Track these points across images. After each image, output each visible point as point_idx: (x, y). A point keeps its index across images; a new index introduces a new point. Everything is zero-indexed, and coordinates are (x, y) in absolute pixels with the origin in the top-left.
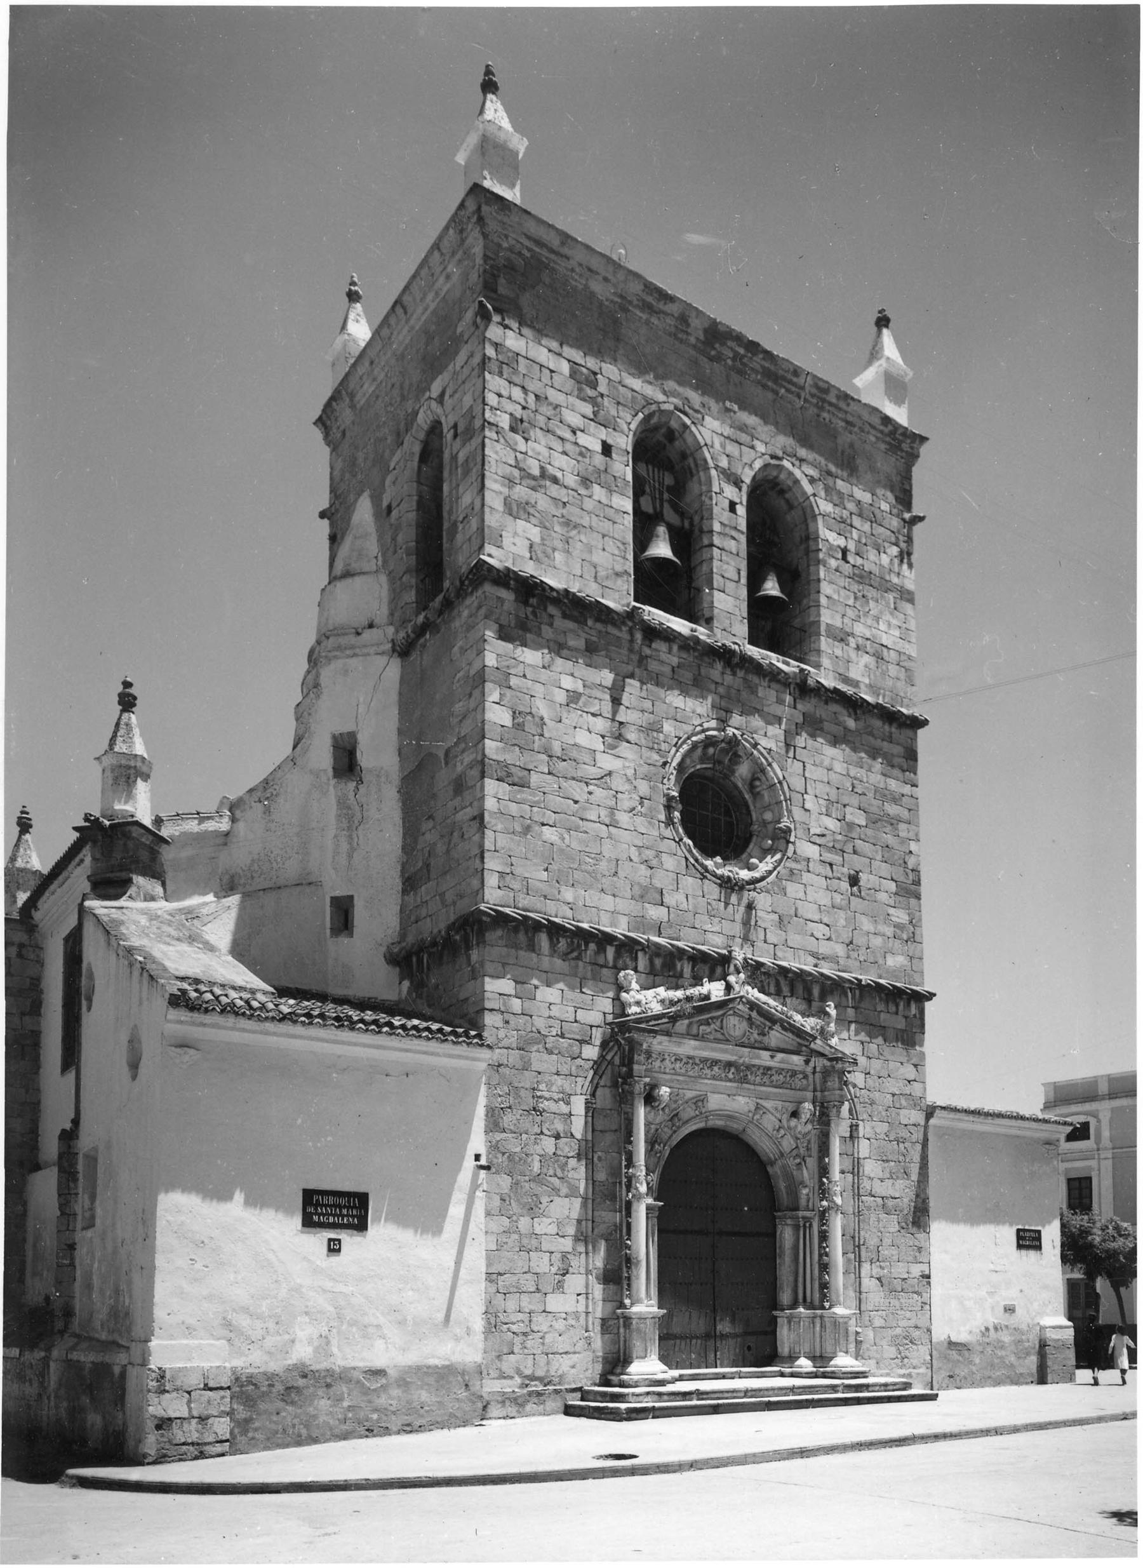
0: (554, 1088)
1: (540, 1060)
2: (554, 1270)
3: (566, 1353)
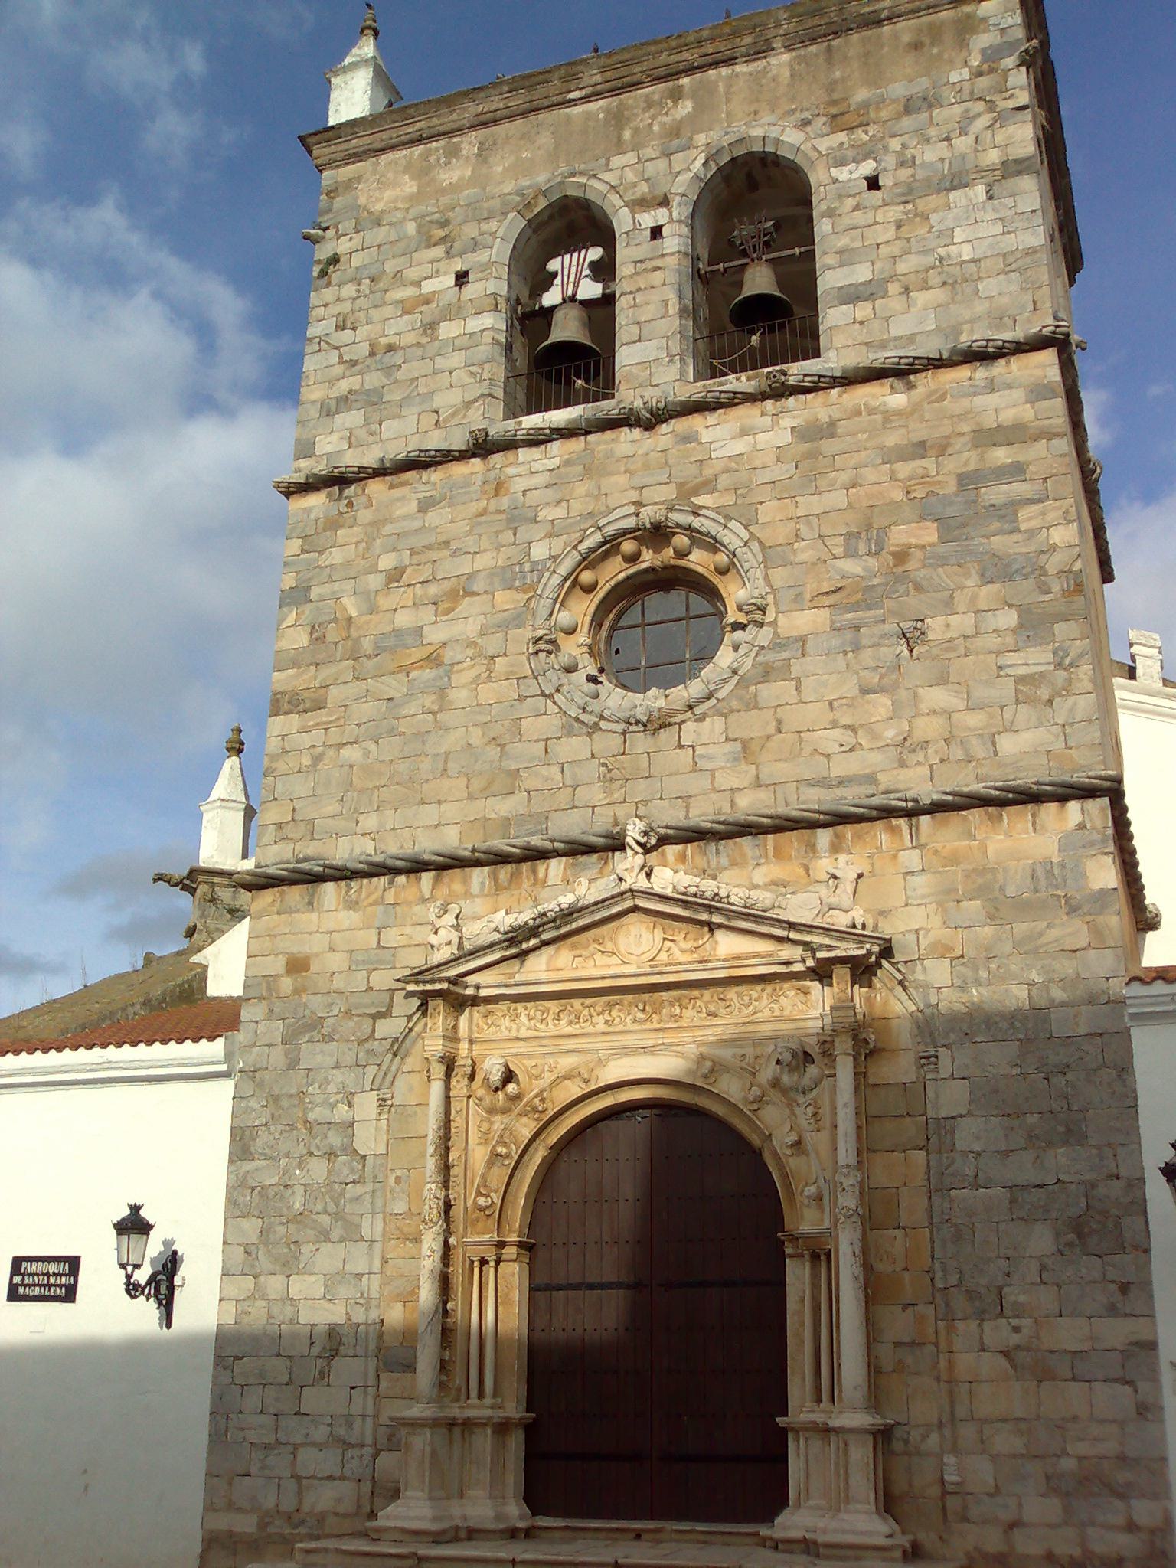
0: (332, 1088)
2: (315, 1350)
3: (330, 1478)
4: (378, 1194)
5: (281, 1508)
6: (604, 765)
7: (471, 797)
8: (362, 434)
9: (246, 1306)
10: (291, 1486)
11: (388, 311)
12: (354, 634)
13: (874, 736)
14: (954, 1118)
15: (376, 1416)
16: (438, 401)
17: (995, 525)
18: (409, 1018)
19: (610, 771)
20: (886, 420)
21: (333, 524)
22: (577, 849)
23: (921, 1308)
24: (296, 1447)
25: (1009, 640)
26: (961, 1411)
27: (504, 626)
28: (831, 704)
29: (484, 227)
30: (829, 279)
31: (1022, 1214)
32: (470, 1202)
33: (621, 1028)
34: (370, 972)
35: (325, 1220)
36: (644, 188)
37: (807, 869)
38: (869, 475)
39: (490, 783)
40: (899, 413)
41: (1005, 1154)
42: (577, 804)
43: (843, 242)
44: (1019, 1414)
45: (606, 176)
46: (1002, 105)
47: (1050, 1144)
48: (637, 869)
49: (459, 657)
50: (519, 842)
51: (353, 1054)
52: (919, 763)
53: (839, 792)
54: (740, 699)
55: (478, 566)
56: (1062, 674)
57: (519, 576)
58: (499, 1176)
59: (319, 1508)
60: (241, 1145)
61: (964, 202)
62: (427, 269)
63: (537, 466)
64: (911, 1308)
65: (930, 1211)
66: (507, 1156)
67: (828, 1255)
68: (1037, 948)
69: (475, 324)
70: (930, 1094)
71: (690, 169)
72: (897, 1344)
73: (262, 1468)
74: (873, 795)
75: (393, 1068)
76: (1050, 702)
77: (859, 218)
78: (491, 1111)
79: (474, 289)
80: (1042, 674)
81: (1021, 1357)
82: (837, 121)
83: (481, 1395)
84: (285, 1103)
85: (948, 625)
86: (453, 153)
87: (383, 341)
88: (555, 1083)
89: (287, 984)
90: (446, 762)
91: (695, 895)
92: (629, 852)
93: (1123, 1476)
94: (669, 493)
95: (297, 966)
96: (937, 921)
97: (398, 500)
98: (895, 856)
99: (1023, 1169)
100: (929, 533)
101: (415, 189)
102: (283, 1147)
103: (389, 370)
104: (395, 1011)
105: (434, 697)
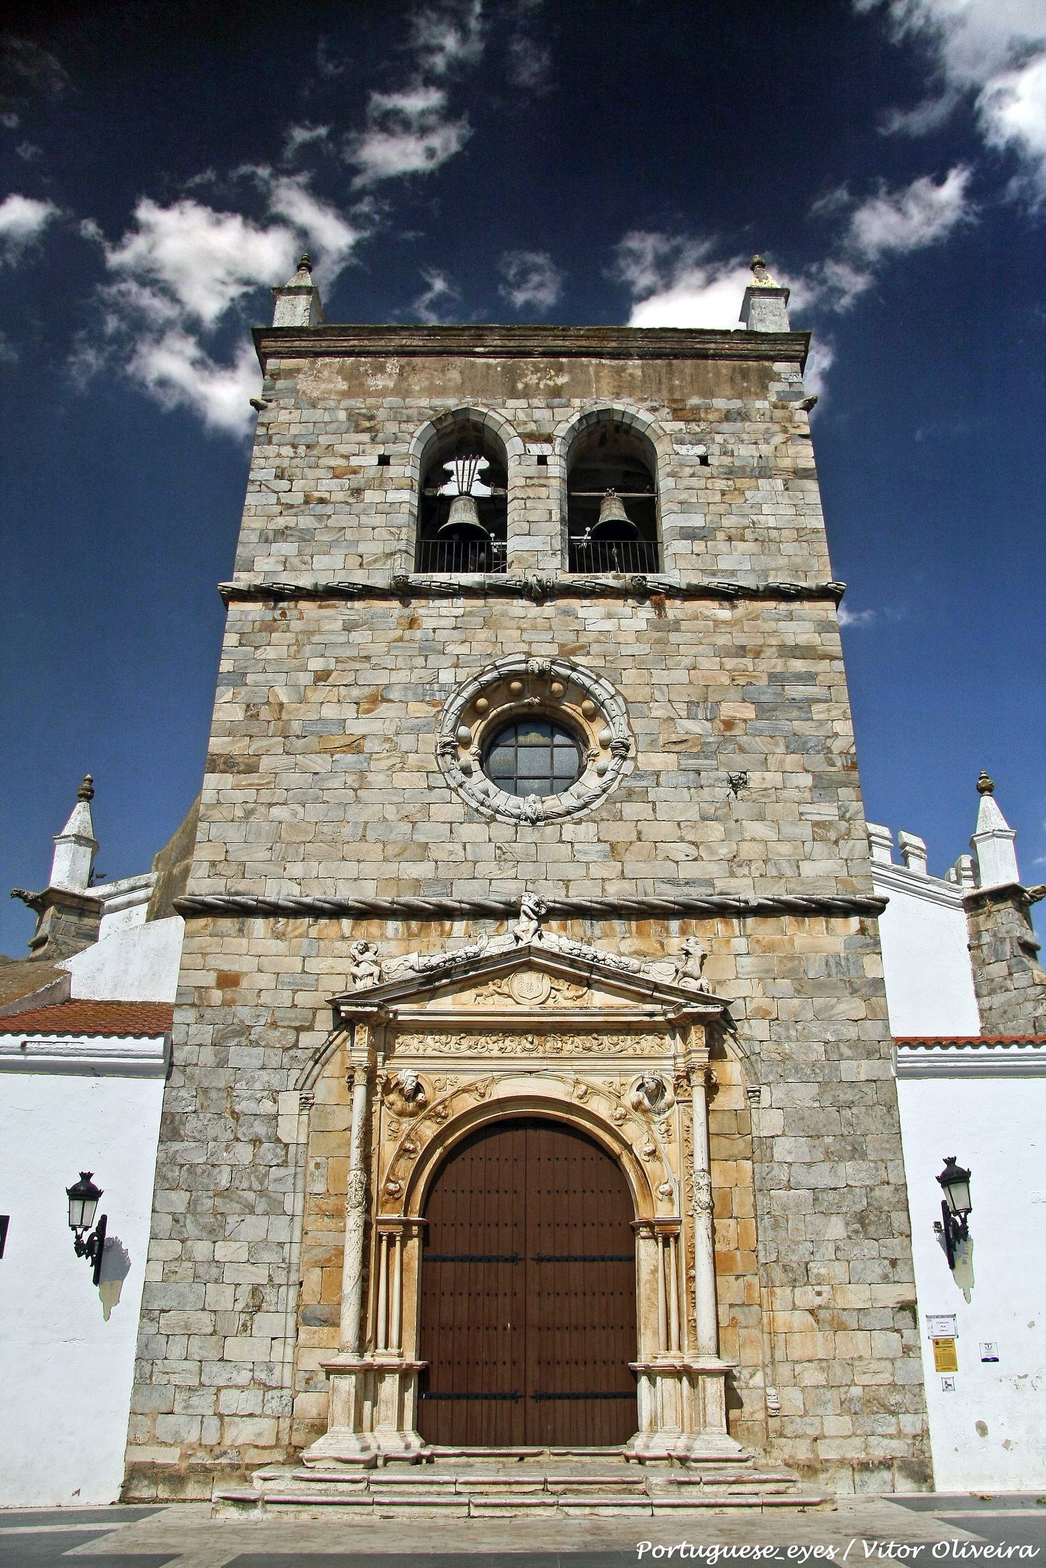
0: (258, 1085)
1: (239, 1055)
2: (239, 1306)
3: (251, 1415)
4: (300, 1176)
5: (204, 1442)
6: (499, 848)
7: (385, 860)
8: (296, 561)
9: (173, 1266)
10: (215, 1422)
11: (320, 473)
12: (285, 716)
13: (712, 852)
14: (773, 1137)
15: (294, 1363)
16: (362, 548)
17: (795, 713)
18: (330, 1033)
19: (504, 853)
20: (715, 626)
21: (269, 627)
22: (479, 912)
23: (749, 1278)
24: (219, 1389)
25: (807, 795)
26: (779, 1355)
27: (415, 730)
28: (679, 825)
29: (404, 426)
30: (668, 521)
31: (822, 1209)
32: (382, 1186)
33: (512, 1055)
34: (295, 992)
35: (250, 1196)
36: (532, 427)
37: (662, 945)
38: (705, 663)
39: (404, 850)
40: (725, 622)
41: (810, 1165)
42: (476, 875)
43: (683, 496)
44: (820, 1356)
45: (503, 411)
46: (792, 431)
47: (841, 1159)
48: (532, 931)
49: (377, 749)
50: (434, 900)
51: (278, 1059)
52: (745, 876)
53: (686, 890)
54: (609, 811)
55: (393, 680)
56: (844, 824)
57: (426, 691)
58: (406, 1167)
59: (240, 1442)
60: (171, 1127)
61: (768, 488)
62: (355, 449)
63: (444, 612)
64: (741, 1279)
65: (755, 1206)
66: (414, 1151)
67: (677, 1238)
68: (830, 1017)
69: (393, 496)
70: (755, 1118)
71: (566, 420)
72: (731, 1305)
73: (185, 1408)
74: (712, 895)
75: (315, 1073)
76: (836, 842)
77: (694, 482)
78: (401, 1114)
79: (393, 471)
80: (831, 823)
81: (823, 1314)
82: (678, 414)
83: (386, 1347)
84: (214, 1095)
85: (764, 779)
86: (381, 369)
87: (317, 494)
88: (455, 1094)
89: (217, 996)
90: (365, 829)
91: (578, 956)
92: (523, 918)
93: (894, 1398)
94: (553, 650)
95: (228, 981)
96: (759, 991)
97: (327, 618)
98: (728, 941)
99: (822, 1176)
100: (749, 712)
101: (345, 387)
102: (211, 1132)
103: (319, 517)
104: (318, 1026)
105: (355, 777)
